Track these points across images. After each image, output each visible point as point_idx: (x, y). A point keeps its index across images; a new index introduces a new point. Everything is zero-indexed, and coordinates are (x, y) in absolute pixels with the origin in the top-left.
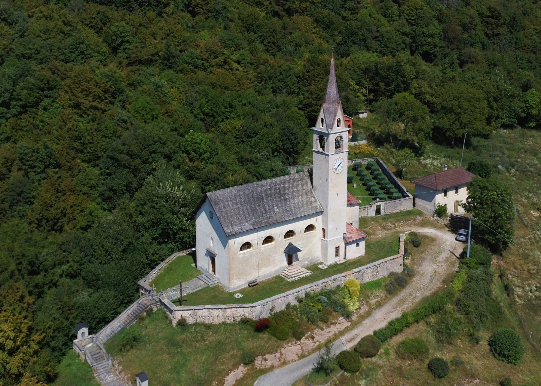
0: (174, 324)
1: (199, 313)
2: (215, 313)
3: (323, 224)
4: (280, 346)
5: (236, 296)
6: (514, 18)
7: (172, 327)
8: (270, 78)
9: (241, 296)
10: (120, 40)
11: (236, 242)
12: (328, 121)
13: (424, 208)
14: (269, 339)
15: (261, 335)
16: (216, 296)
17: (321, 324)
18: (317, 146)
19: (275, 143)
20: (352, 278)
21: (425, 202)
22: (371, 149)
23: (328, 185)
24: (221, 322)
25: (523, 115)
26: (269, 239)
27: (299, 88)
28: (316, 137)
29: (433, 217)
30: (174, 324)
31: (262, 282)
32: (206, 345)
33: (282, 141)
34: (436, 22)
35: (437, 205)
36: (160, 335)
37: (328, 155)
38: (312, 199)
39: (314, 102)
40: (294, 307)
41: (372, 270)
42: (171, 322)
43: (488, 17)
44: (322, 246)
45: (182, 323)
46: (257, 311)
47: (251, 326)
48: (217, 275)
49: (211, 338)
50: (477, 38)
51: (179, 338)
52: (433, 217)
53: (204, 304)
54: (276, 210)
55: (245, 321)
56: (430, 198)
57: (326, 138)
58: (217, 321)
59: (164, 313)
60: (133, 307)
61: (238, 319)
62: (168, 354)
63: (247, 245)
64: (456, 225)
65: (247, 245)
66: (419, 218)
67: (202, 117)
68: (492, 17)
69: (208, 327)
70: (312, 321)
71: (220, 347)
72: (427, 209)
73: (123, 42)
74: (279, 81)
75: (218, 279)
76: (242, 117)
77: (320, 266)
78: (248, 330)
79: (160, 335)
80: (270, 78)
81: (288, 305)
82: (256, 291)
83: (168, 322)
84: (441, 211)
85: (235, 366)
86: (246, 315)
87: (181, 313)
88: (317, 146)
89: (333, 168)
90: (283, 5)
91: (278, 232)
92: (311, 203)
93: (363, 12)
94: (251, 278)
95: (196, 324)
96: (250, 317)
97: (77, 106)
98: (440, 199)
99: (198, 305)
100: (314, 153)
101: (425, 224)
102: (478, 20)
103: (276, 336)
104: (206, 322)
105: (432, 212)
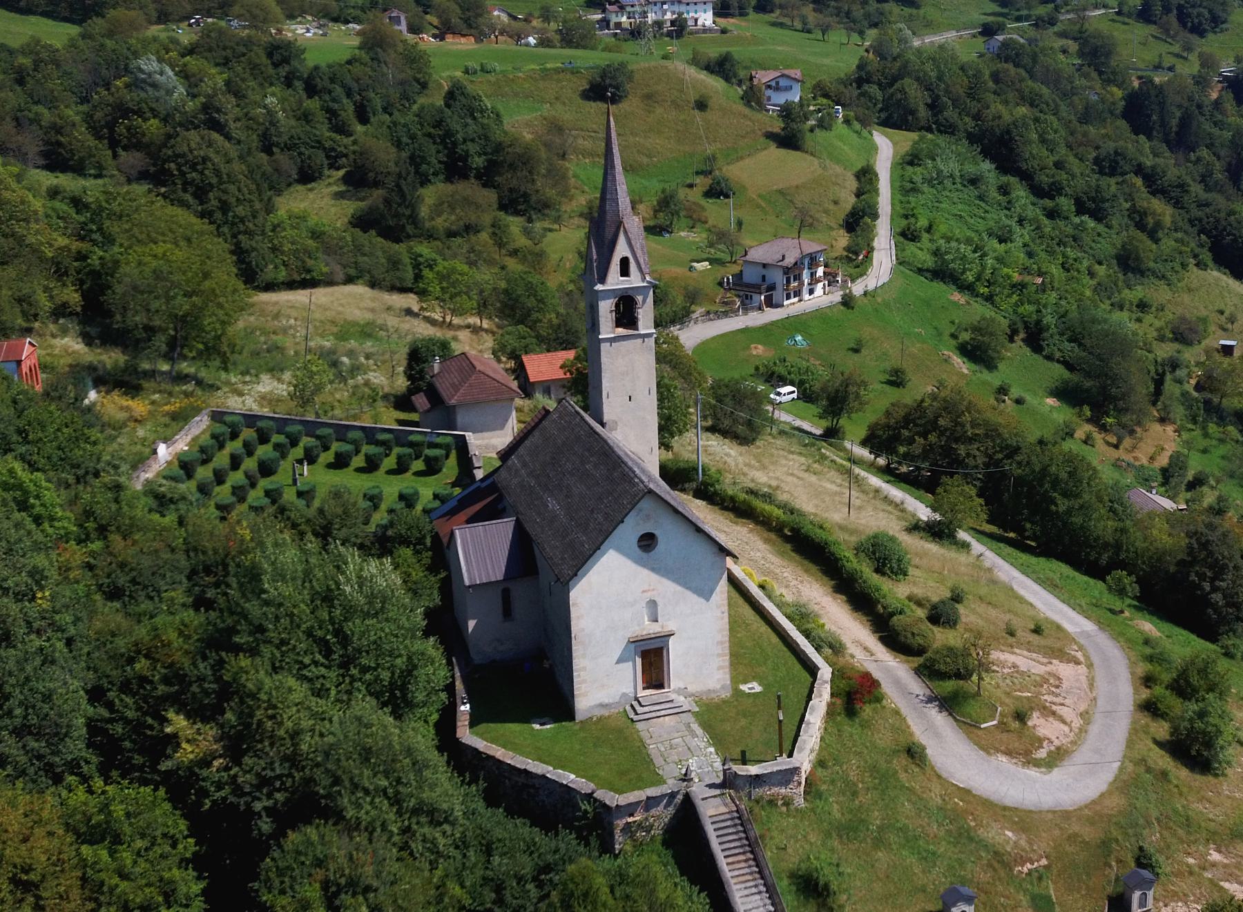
0: (800, 802)
21: (486, 434)
42: (788, 802)
75: (682, 691)
83: (784, 809)
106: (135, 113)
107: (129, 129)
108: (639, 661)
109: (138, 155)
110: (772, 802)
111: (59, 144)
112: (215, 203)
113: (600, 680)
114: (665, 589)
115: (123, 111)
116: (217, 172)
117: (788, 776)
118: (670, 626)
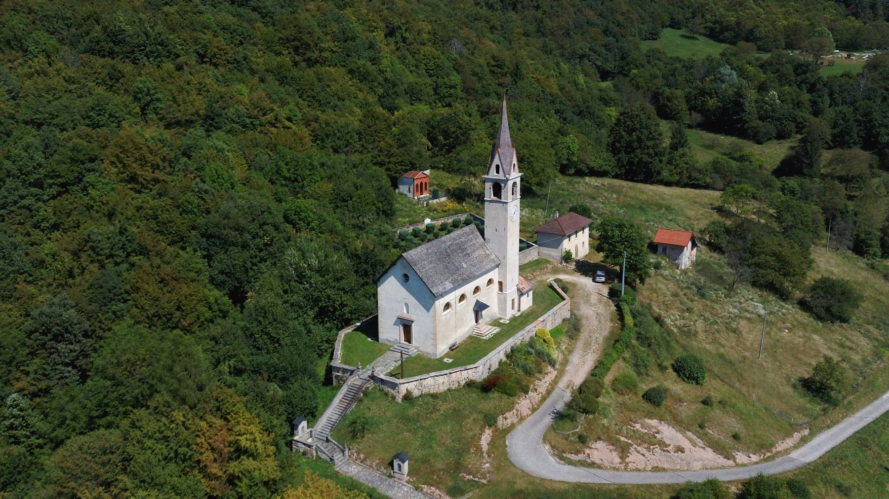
0: (399, 400)
1: (425, 382)
2: (441, 380)
3: (500, 277)
4: (513, 403)
5: (445, 360)
6: (517, 67)
7: (397, 403)
8: (327, 136)
9: (451, 361)
10: (149, 98)
11: (440, 303)
12: (505, 167)
13: (549, 255)
14: (501, 398)
15: (490, 395)
16: (427, 365)
17: (536, 375)
18: (489, 195)
19: (374, 204)
20: (540, 327)
21: (550, 249)
22: (452, 205)
23: (506, 234)
24: (446, 389)
25: (565, 162)
26: (463, 297)
27: (363, 146)
28: (488, 186)
29: (561, 263)
30: (399, 400)
31: (461, 344)
32: (442, 415)
33: (382, 202)
34: (455, 73)
35: (564, 250)
36: (388, 414)
37: (506, 203)
38: (488, 252)
39: (387, 160)
40: (505, 363)
41: (550, 318)
42: (394, 398)
43: (493, 66)
44: (499, 299)
45: (408, 397)
46: (479, 371)
47: (477, 387)
48: (414, 343)
49: (444, 407)
50: (490, 87)
51: (412, 412)
52: (561, 263)
53: (428, 372)
54: (465, 266)
55: (470, 384)
56: (557, 244)
57: (503, 185)
58: (443, 388)
59: (381, 390)
60: (344, 390)
61: (463, 383)
62: (410, 431)
63: (447, 306)
64: (585, 268)
65: (447, 306)
66: (550, 266)
67: (284, 182)
68: (497, 66)
69: (434, 396)
70: (528, 372)
71: (457, 414)
72: (553, 257)
73: (152, 100)
74: (339, 139)
75: (416, 348)
76: (326, 179)
77: (501, 321)
78: (475, 392)
79: (388, 414)
80: (327, 136)
81: (500, 363)
82: (468, 351)
84: (567, 257)
85: (482, 430)
86: (471, 377)
87: (409, 386)
88: (489, 195)
89: (509, 215)
90: (304, 54)
91: (468, 289)
92: (488, 256)
93: (385, 62)
94: (451, 342)
95: (421, 396)
96: (474, 378)
97: (133, 179)
98: (568, 245)
99: (411, 376)
100: (486, 204)
101: (555, 271)
102: (487, 69)
103: (507, 394)
104: (432, 392)
105: (559, 258)
106: (707, 94)
107: (702, 102)
108: (402, 328)
109: (699, 115)
110: (386, 394)
111: (667, 106)
112: (635, 137)
113: (388, 331)
114: (412, 301)
115: (703, 93)
116: (641, 122)
117: (394, 386)
118: (413, 318)
